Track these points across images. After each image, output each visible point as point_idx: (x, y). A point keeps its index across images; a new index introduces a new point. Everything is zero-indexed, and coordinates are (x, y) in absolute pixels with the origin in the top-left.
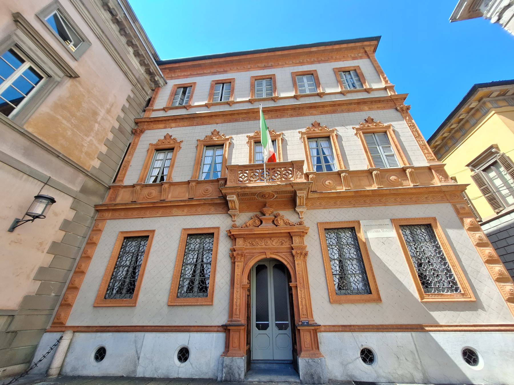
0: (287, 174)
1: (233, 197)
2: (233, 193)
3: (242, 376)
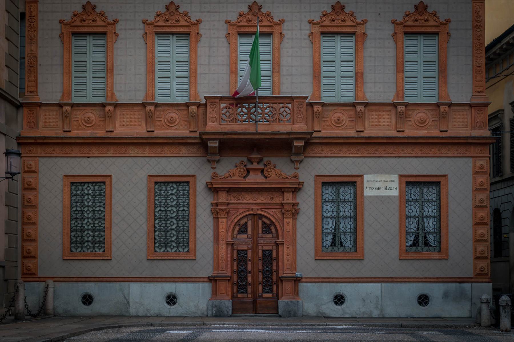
0: (285, 113)
1: (216, 143)
3: (230, 313)
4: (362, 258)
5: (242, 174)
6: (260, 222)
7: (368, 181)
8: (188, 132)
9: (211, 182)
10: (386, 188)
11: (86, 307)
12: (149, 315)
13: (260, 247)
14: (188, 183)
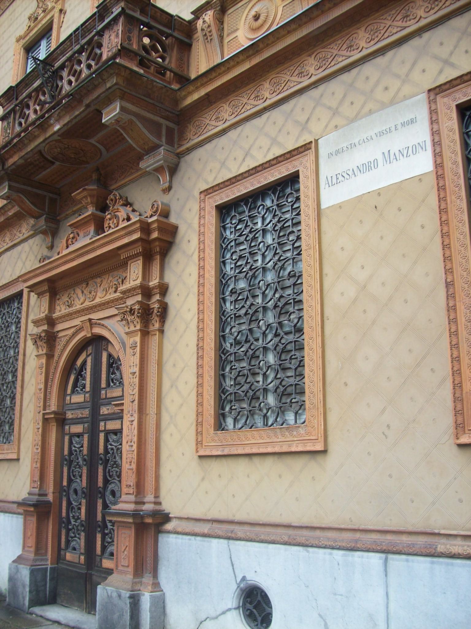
4: (319, 447)
10: (388, 157)
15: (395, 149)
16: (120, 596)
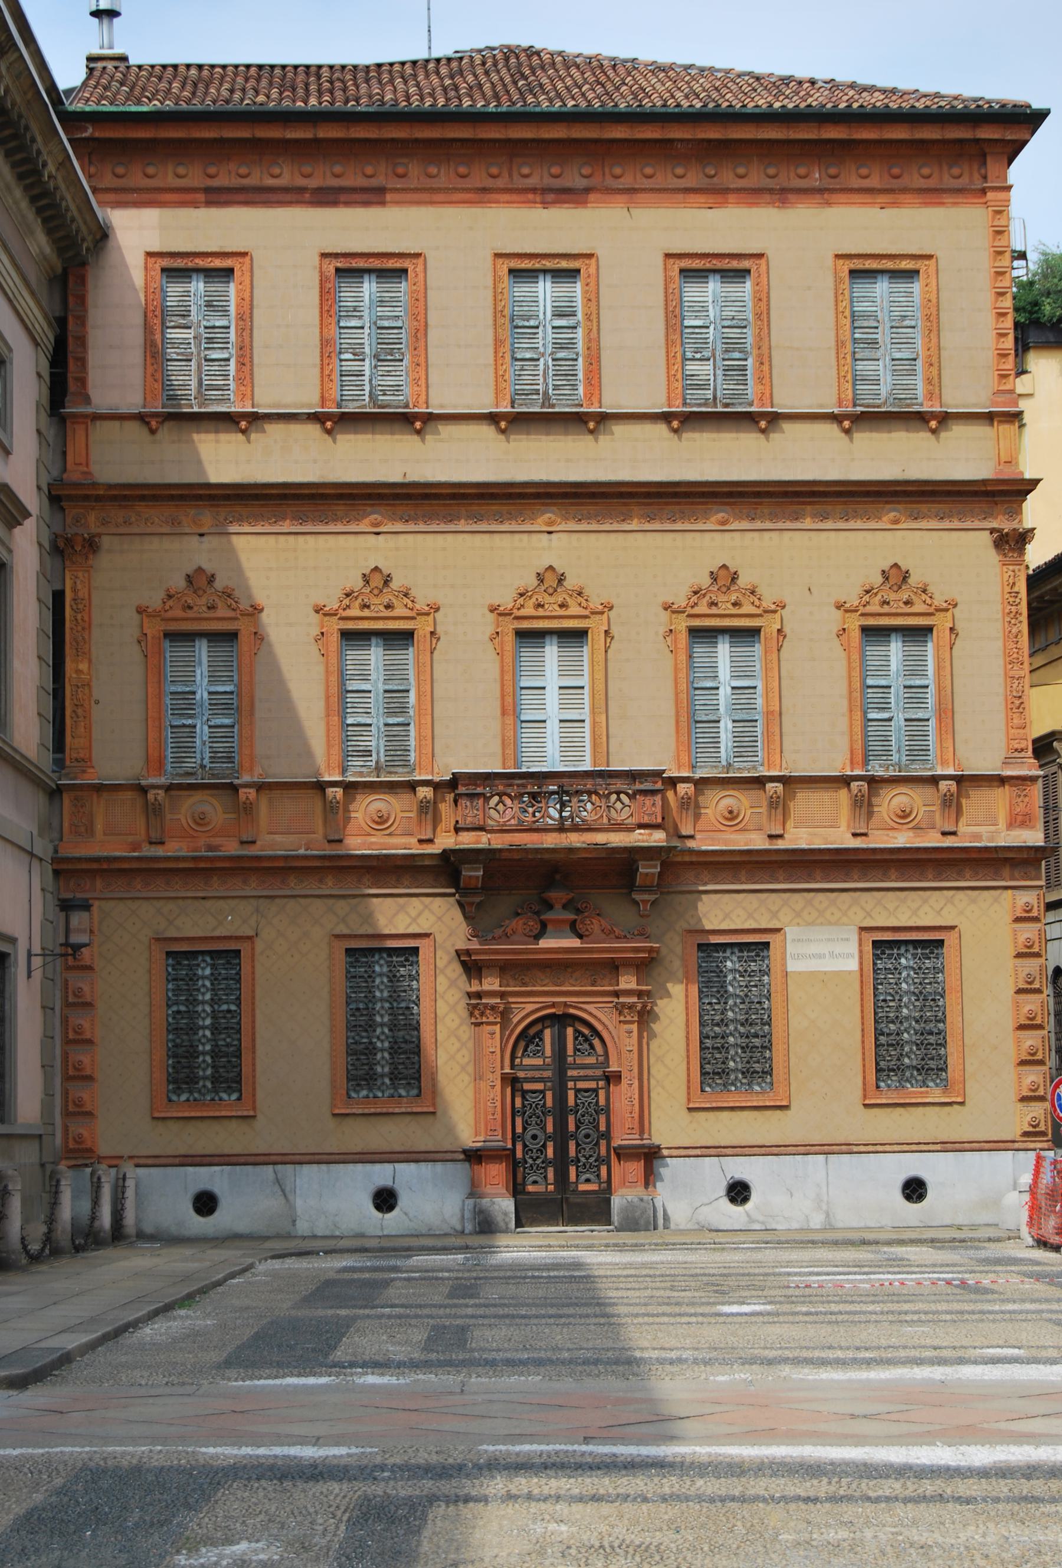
2: (476, 862)
4: (784, 1103)
5: (531, 930)
6: (570, 1031)
7: (794, 940)
8: (413, 841)
9: (468, 950)
10: (832, 954)
11: (201, 1219)
12: (337, 1233)
13: (571, 1084)
14: (415, 951)
15: (836, 952)
16: (642, 1200)
